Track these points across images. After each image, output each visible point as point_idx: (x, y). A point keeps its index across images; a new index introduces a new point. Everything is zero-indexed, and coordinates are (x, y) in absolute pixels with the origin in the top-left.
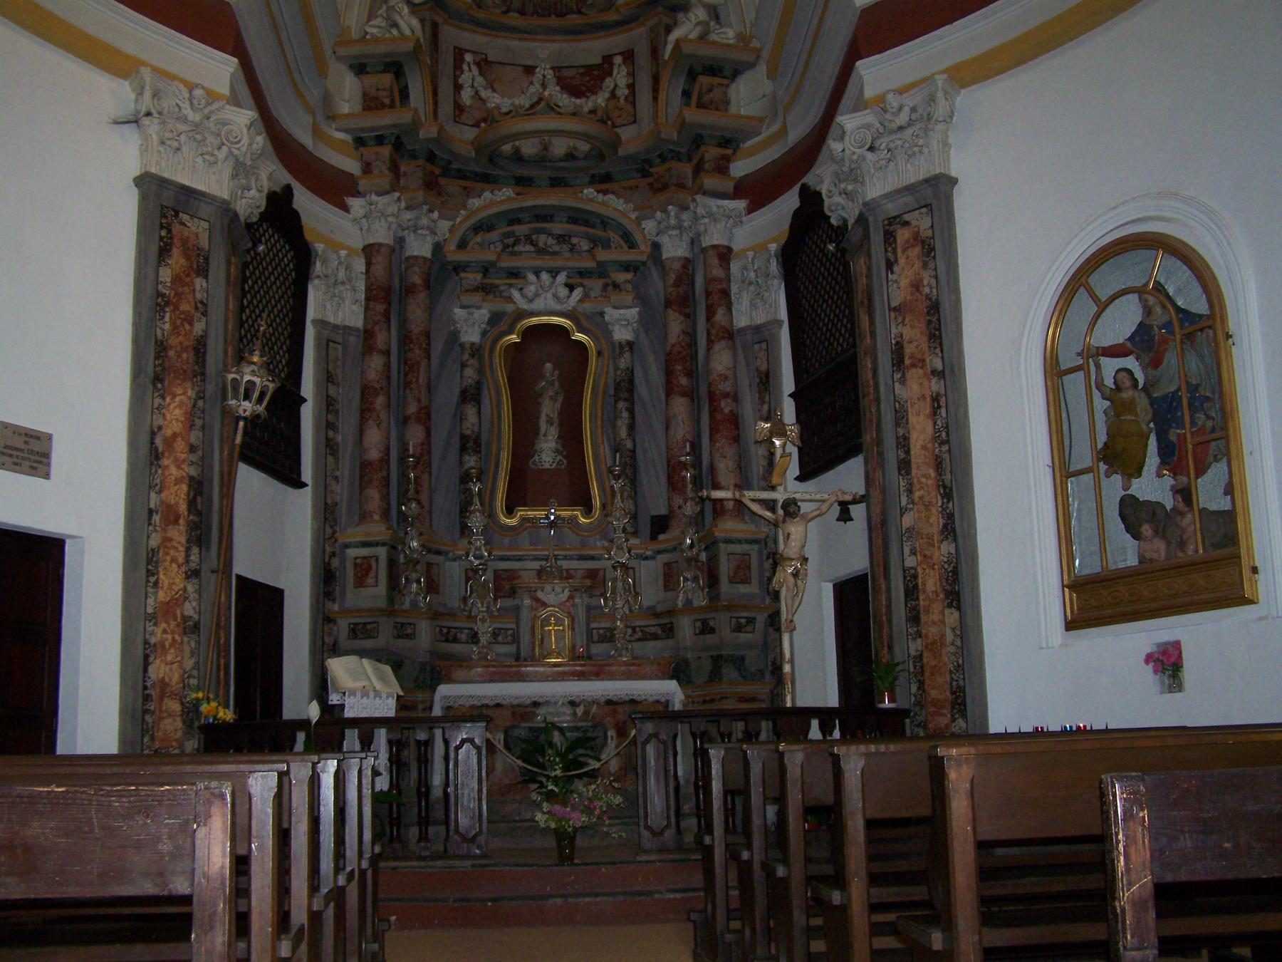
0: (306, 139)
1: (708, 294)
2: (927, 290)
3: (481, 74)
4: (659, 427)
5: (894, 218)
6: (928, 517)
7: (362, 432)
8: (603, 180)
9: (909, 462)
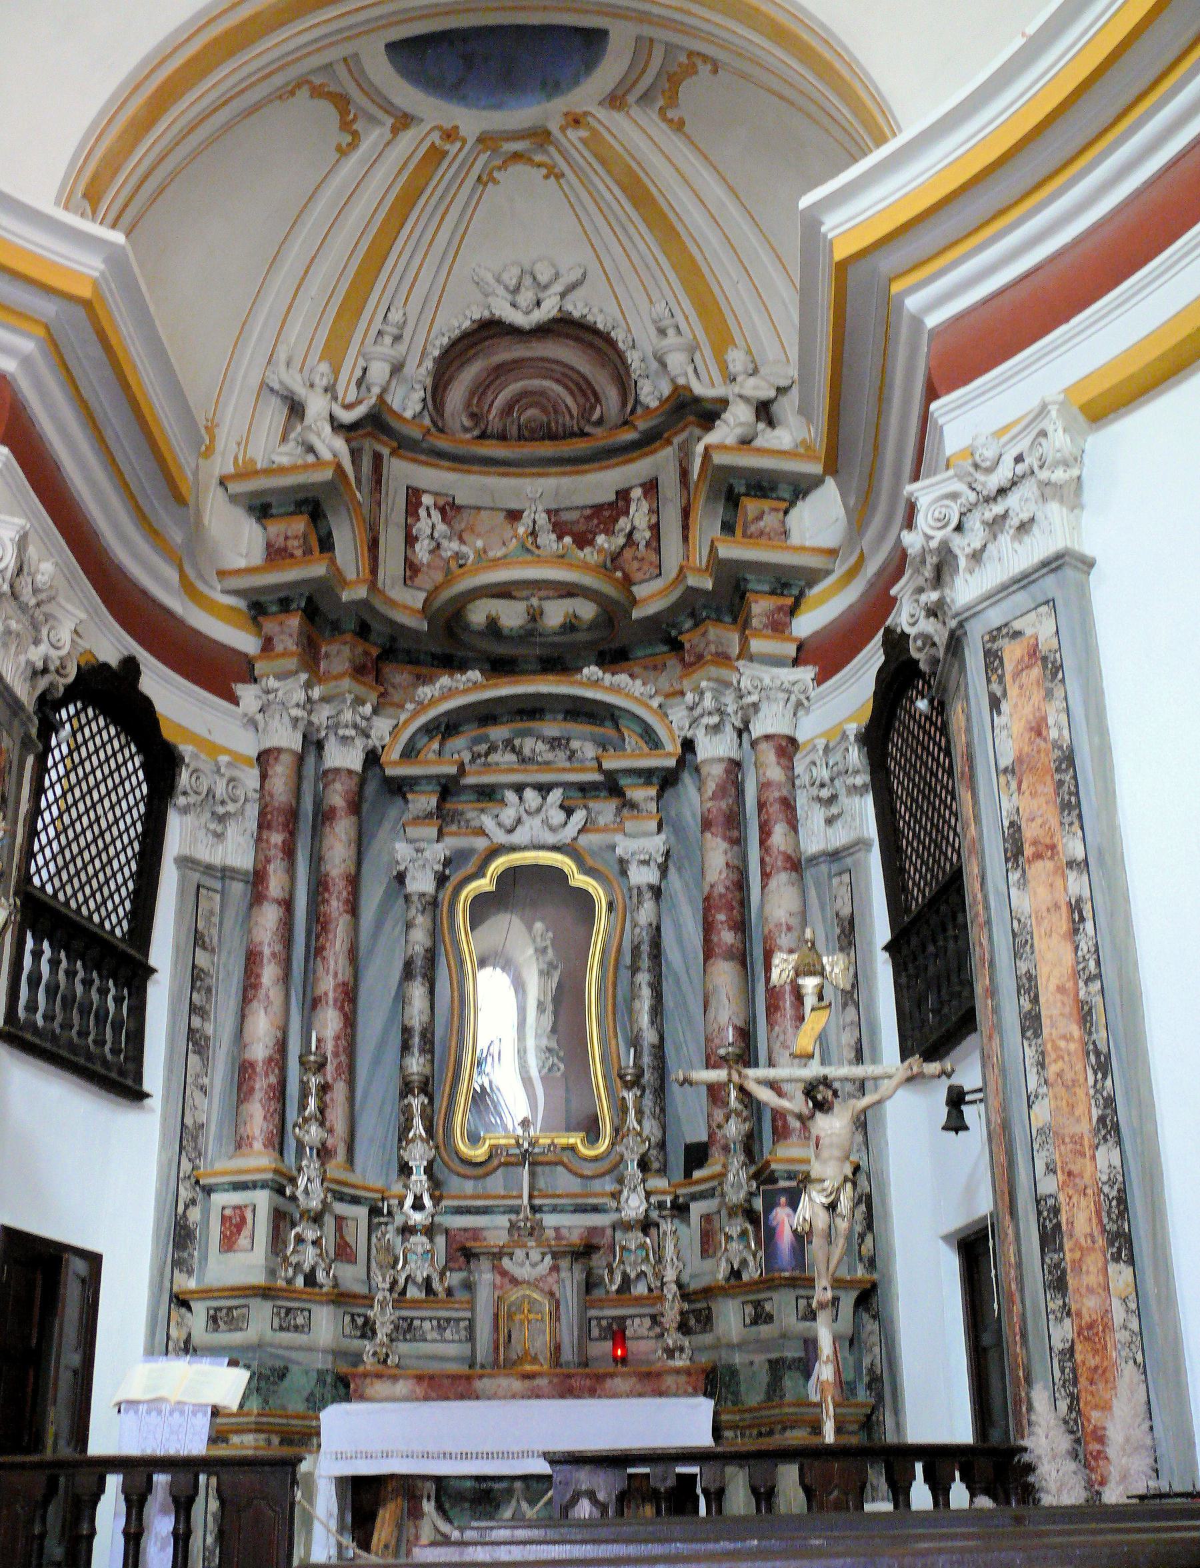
0: (176, 603)
1: (761, 806)
2: (1053, 734)
3: (444, 519)
4: (696, 1008)
5: (999, 629)
6: (1072, 1107)
7: (242, 1017)
8: (614, 657)
9: (1038, 1017)
